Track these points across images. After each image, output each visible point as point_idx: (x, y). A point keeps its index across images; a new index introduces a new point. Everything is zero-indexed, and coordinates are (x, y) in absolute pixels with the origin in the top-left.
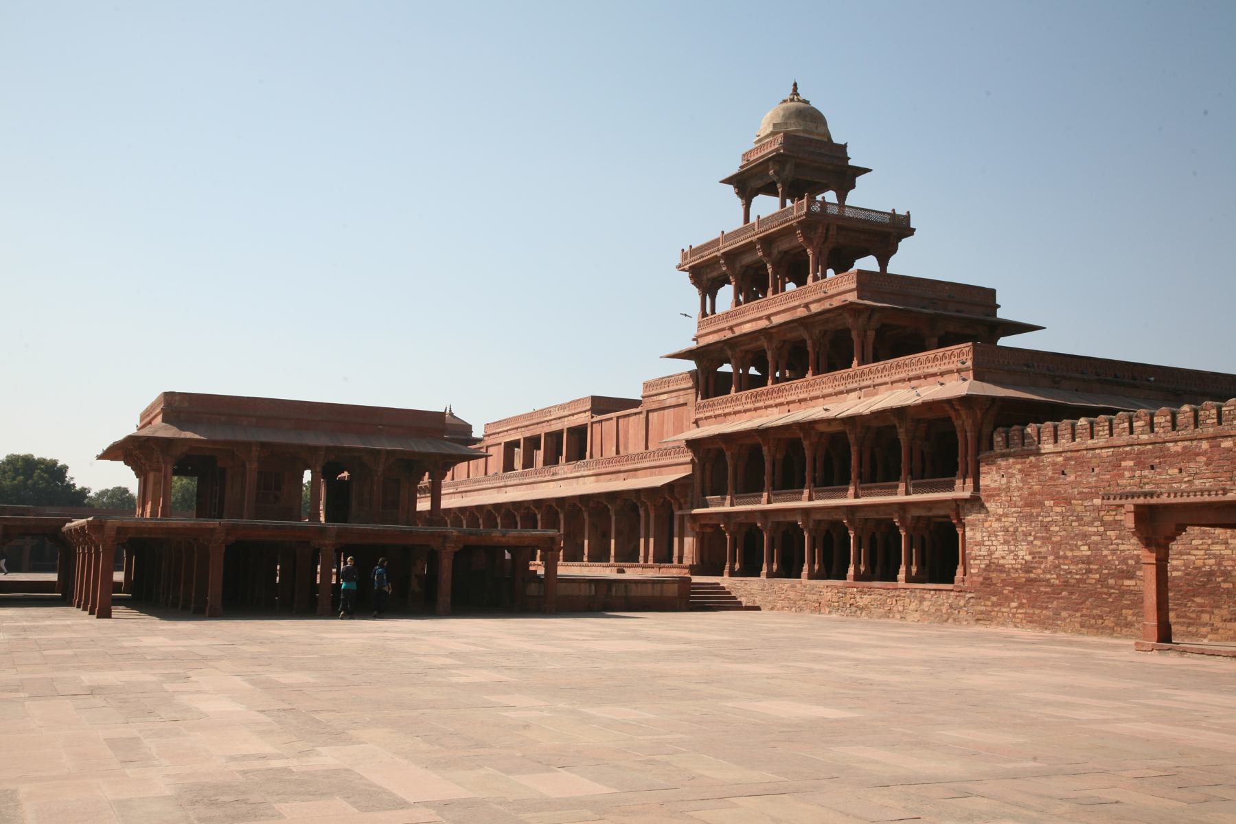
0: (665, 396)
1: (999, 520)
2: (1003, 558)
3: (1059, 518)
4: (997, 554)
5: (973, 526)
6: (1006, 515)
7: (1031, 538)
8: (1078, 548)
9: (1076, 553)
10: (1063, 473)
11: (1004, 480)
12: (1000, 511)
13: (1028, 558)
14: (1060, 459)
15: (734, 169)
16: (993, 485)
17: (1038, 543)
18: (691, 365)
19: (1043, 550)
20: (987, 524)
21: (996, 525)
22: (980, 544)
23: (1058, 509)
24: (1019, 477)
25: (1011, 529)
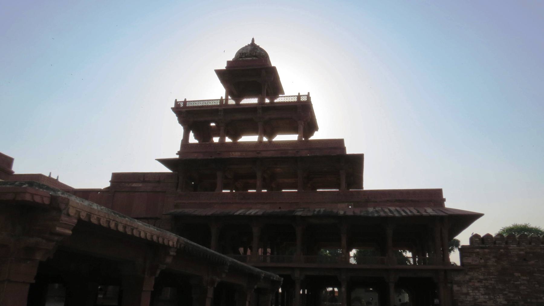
0: (140, 185)
1: (480, 281)
2: (485, 302)
3: (526, 282)
4: (480, 300)
5: (459, 284)
6: (486, 279)
7: (506, 292)
8: (541, 298)
9: (540, 301)
10: (525, 260)
11: (483, 261)
12: (481, 277)
13: (505, 302)
14: (522, 253)
15: (223, 66)
16: (474, 263)
17: (512, 295)
18: (165, 170)
19: (517, 298)
20: (471, 284)
21: (477, 284)
22: (467, 294)
23: (525, 278)
24: (494, 260)
25: (490, 287)
